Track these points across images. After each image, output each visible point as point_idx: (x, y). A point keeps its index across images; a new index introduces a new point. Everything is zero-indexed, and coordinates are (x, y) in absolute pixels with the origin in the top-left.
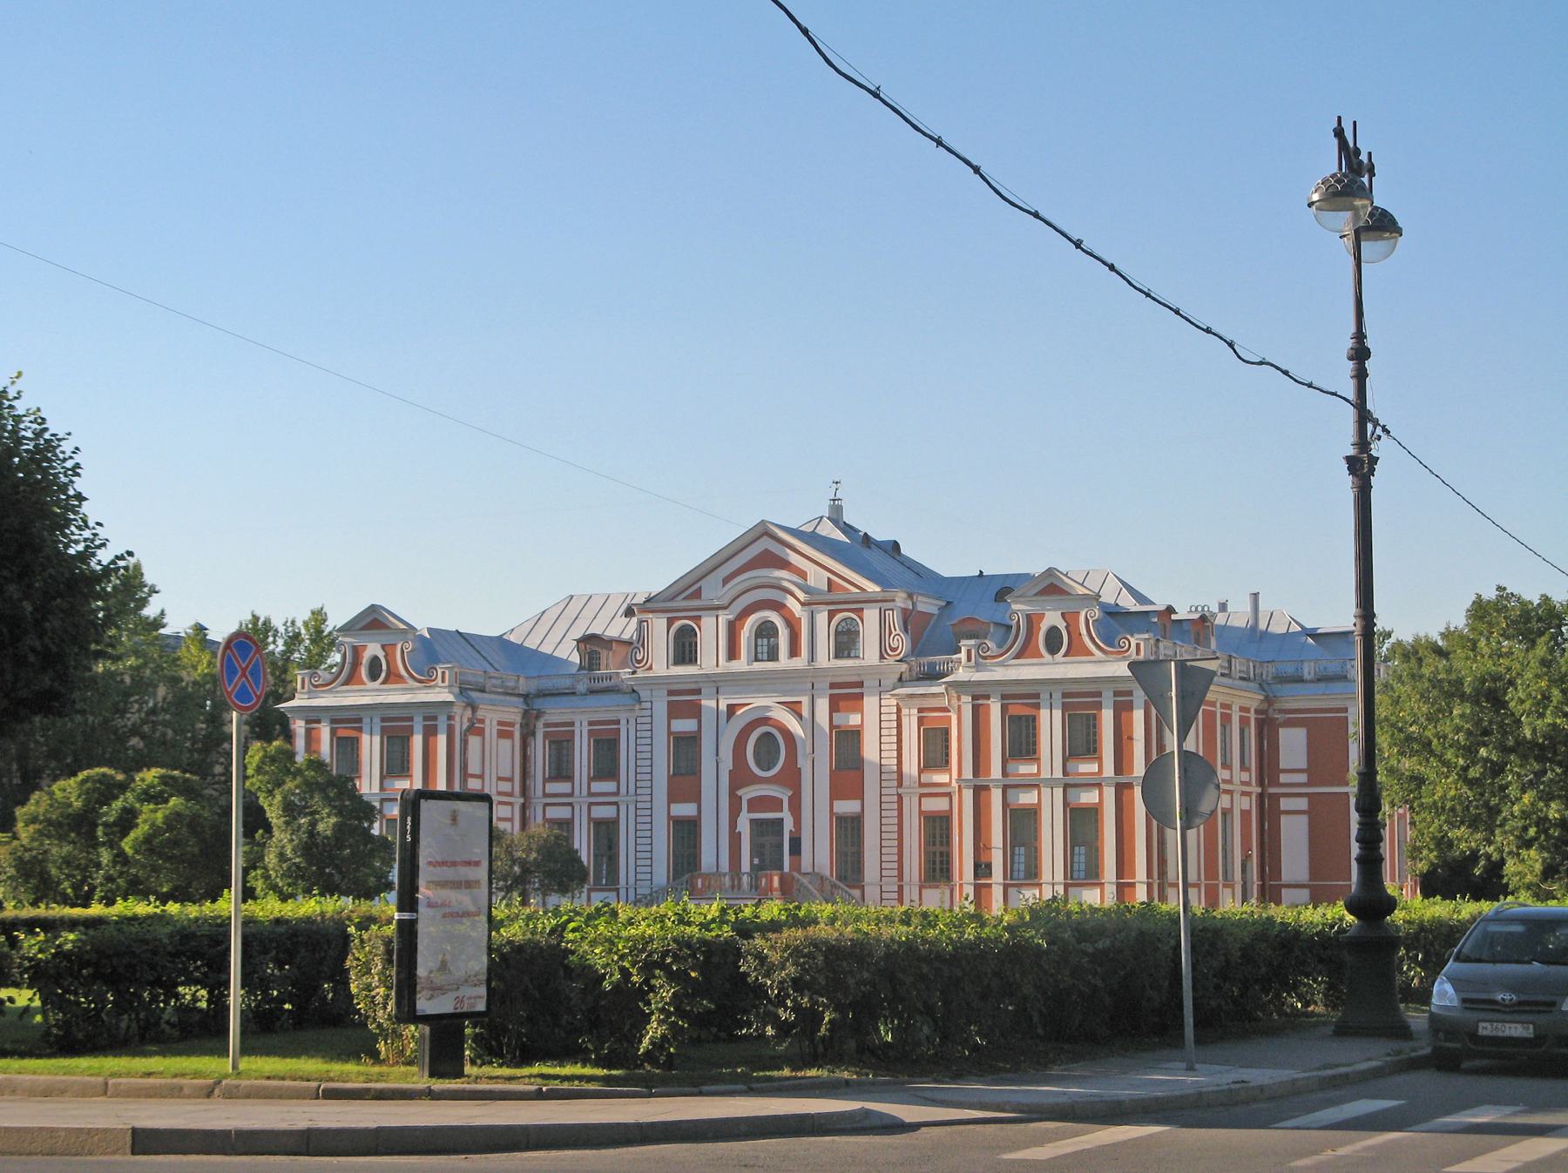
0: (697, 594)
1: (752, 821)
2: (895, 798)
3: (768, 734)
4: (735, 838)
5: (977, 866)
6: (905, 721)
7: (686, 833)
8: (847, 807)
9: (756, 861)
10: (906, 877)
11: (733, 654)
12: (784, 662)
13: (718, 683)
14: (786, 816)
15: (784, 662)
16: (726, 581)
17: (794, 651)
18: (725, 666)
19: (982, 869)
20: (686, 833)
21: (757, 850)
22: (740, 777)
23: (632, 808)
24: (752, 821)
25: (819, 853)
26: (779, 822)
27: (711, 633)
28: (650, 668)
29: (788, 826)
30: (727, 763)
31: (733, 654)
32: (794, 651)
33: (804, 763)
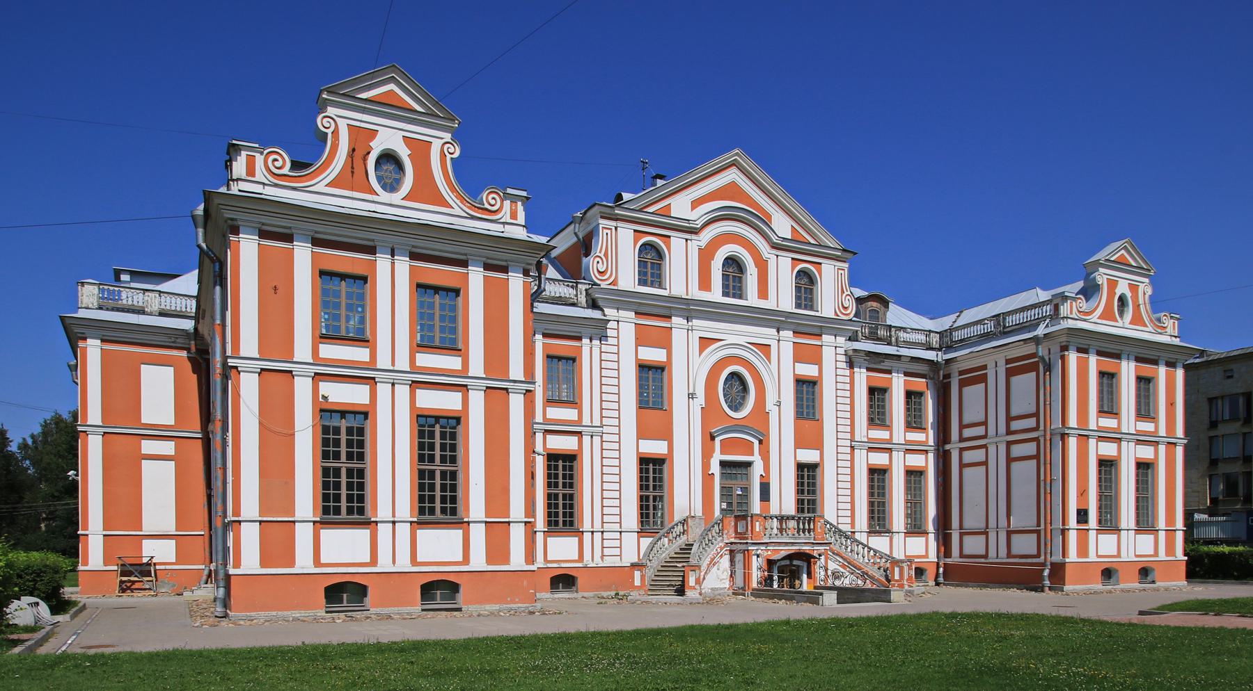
0: (665, 212)
1: (723, 464)
2: (848, 450)
3: (734, 376)
4: (708, 477)
5: (1079, 512)
6: (857, 376)
7: (653, 471)
8: (809, 456)
9: (724, 506)
10: (857, 528)
11: (705, 284)
12: (752, 298)
13: (690, 309)
14: (756, 459)
15: (752, 298)
16: (695, 204)
17: (763, 293)
18: (696, 294)
19: (1082, 515)
20: (653, 471)
21: (726, 493)
22: (709, 412)
23: (597, 440)
24: (723, 464)
25: (785, 499)
26: (748, 465)
27: (681, 259)
28: (614, 283)
29: (758, 469)
30: (700, 400)
31: (705, 284)
32: (763, 293)
33: (770, 406)
